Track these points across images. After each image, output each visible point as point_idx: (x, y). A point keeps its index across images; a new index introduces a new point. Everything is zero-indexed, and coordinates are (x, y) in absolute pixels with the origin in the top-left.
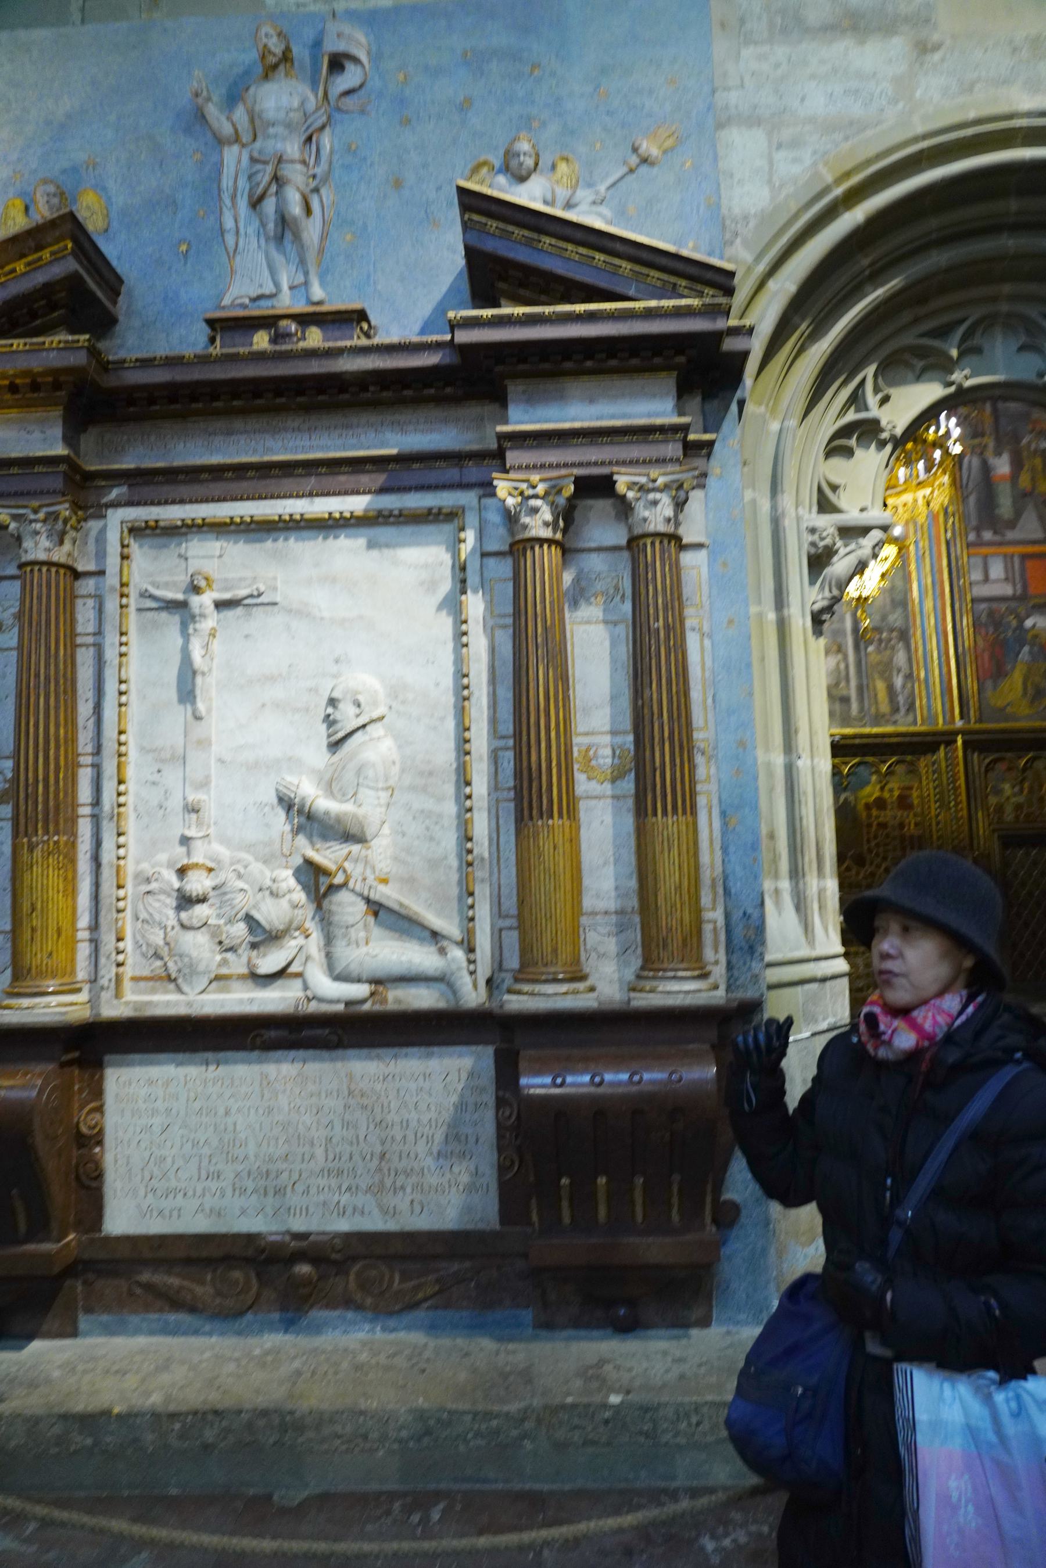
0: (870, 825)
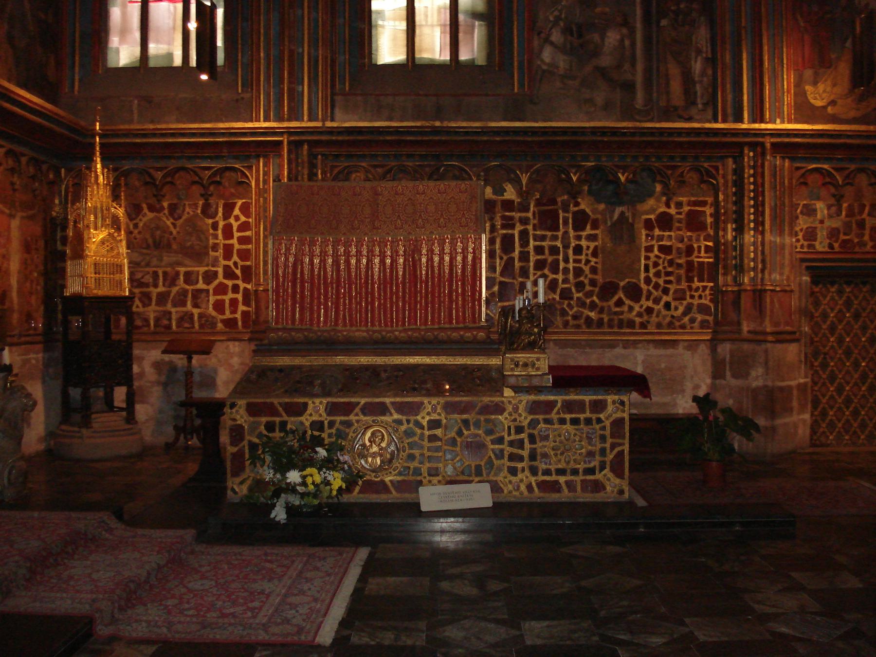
0: (649, 249)
